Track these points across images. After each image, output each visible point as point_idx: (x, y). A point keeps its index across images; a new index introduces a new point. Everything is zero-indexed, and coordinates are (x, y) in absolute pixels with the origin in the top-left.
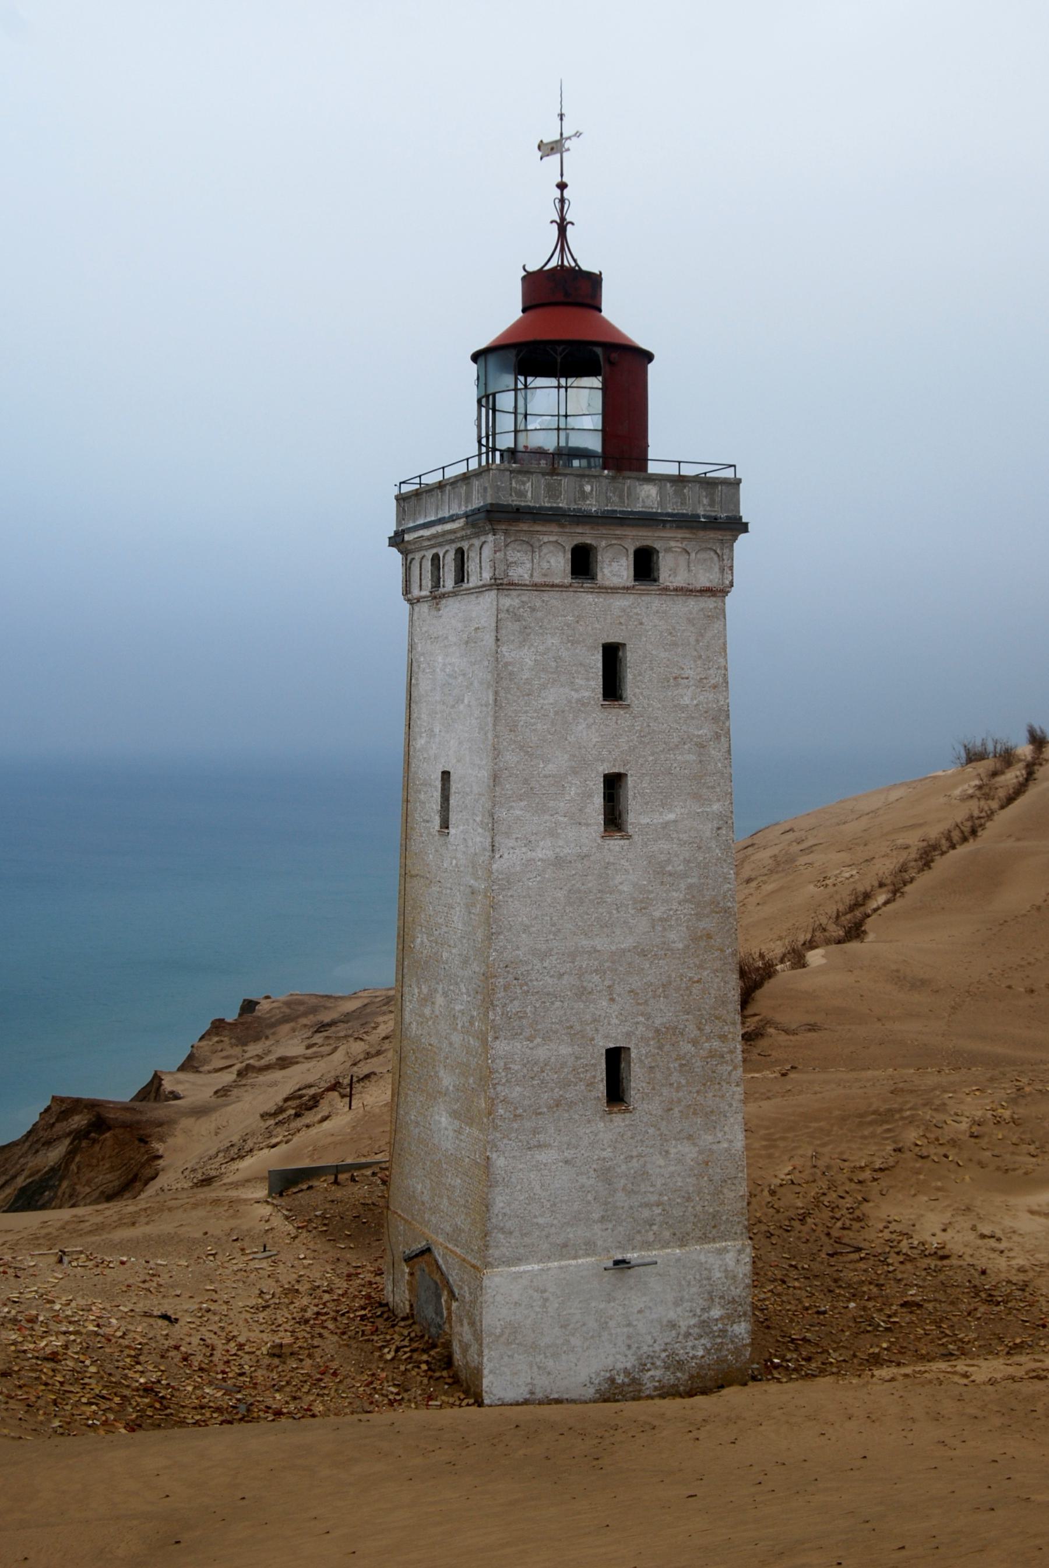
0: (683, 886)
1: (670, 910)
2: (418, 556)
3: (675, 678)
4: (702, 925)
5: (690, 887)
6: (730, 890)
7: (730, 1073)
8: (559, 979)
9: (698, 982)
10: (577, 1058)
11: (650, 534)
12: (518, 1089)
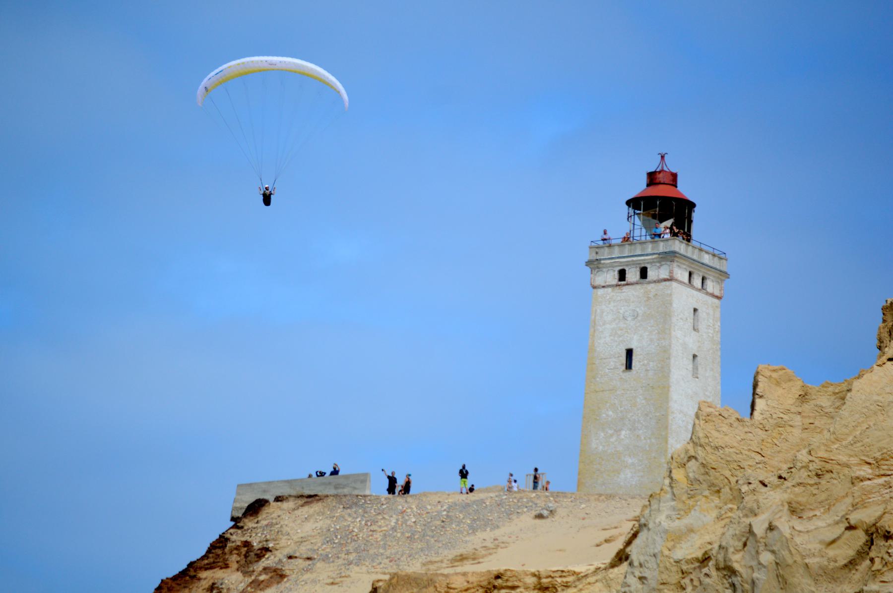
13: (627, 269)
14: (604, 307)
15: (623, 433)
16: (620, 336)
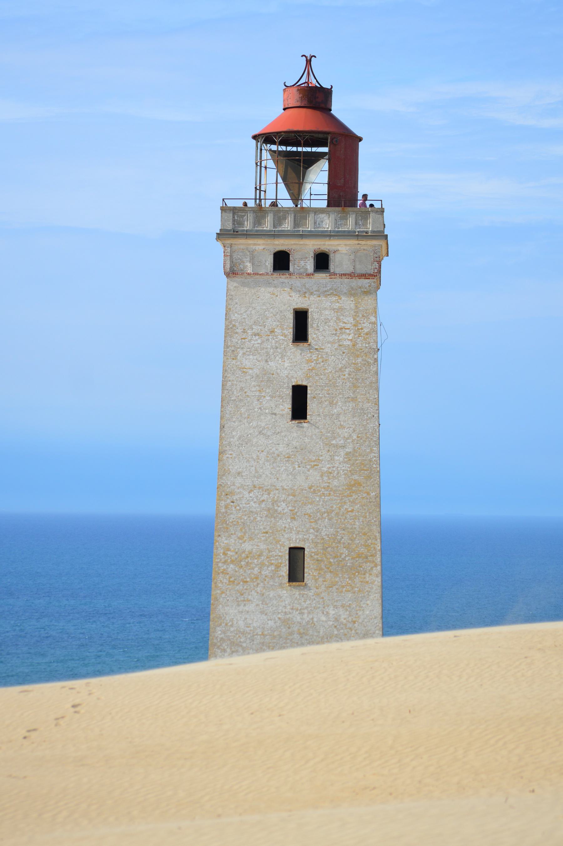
0: (342, 453)
1: (333, 467)
3: (341, 329)
4: (356, 477)
5: (347, 454)
6: (375, 457)
7: (372, 568)
8: (259, 504)
9: (351, 511)
10: (269, 551)
11: (323, 243)
12: (232, 566)
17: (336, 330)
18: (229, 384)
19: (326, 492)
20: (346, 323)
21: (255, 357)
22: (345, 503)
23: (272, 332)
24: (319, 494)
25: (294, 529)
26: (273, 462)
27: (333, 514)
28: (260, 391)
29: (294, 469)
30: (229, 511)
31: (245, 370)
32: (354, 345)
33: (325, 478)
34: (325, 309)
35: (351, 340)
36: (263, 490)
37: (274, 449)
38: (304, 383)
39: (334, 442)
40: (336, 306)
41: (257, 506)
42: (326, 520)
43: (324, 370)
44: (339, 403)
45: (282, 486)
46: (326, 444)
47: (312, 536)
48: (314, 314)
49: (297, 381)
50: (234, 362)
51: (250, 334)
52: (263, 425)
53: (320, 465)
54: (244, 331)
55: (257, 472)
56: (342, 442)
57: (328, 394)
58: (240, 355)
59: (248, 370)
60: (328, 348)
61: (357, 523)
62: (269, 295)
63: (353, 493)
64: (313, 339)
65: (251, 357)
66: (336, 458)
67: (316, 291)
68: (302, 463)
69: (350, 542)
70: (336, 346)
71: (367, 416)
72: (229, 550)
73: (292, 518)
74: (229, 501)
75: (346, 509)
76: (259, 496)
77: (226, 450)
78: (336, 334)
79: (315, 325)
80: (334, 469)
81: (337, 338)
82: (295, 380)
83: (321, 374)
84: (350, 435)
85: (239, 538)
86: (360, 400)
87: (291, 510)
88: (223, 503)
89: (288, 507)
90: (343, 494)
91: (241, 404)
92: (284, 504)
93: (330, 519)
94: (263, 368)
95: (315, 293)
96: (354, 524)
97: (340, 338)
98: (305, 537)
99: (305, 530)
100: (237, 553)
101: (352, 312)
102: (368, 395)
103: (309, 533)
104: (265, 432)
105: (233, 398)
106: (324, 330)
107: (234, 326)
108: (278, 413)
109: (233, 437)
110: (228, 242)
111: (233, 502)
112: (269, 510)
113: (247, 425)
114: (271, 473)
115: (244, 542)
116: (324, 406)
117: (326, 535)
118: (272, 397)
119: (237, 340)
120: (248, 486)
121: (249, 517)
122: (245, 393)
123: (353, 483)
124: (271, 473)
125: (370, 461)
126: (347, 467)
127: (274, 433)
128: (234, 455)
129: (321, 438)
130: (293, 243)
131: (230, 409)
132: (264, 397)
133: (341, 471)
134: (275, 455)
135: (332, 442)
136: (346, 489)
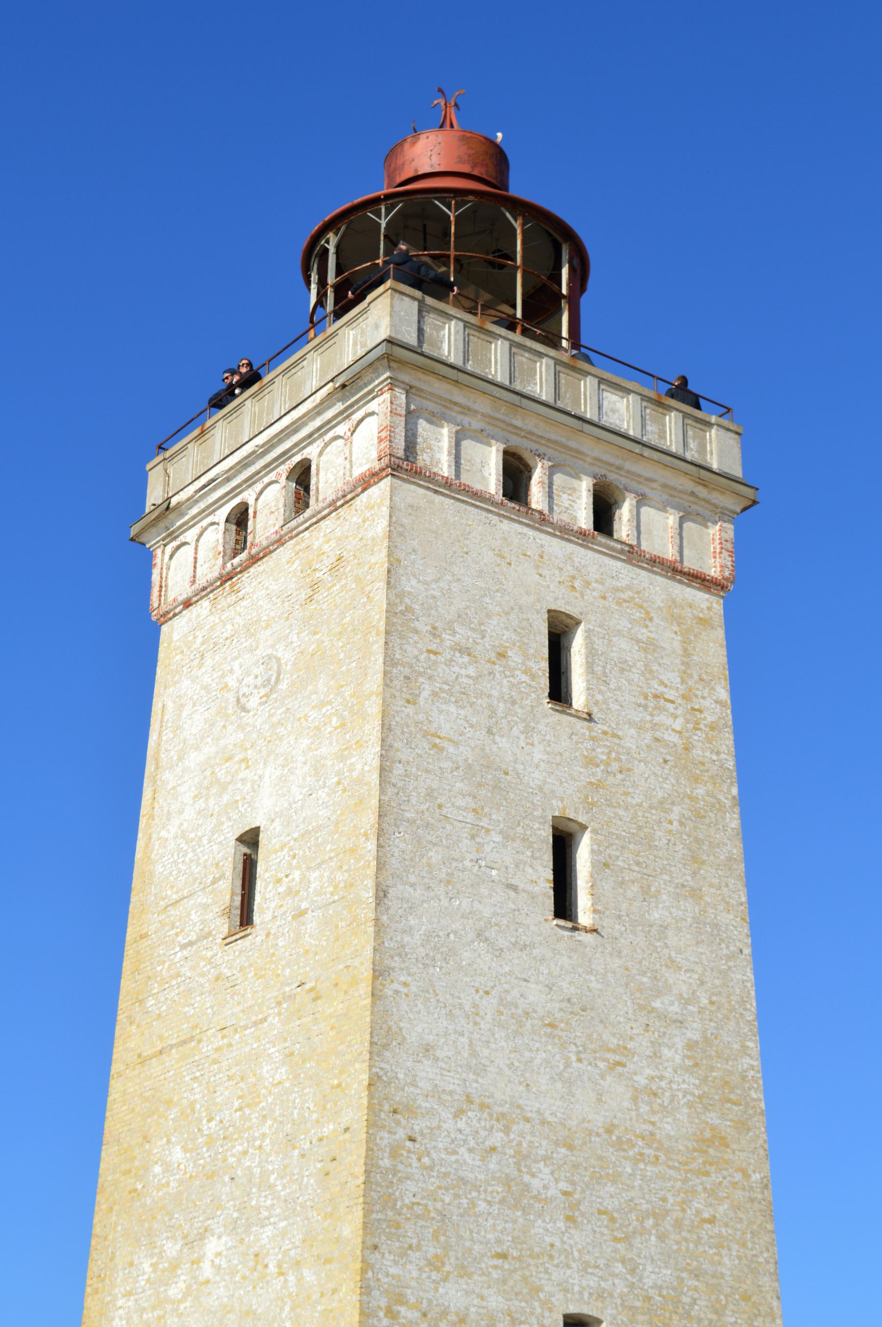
0: (679, 1042)
1: (661, 1078)
2: (190, 535)
3: (656, 696)
4: (713, 1118)
5: (691, 1045)
13: (251, 502)
14: (186, 683)
15: (212, 1246)
16: (224, 788)
17: (646, 698)
18: (398, 770)
19: (647, 1151)
20: (666, 686)
21: (462, 712)
22: (694, 1192)
23: (502, 655)
24: (631, 1153)
25: (576, 1254)
26: (516, 1033)
27: (667, 1224)
28: (474, 810)
29: (567, 1065)
30: (400, 1167)
31: (438, 741)
32: (687, 749)
33: (644, 1109)
34: (619, 633)
35: (680, 732)
36: (491, 1115)
37: (515, 993)
38: (582, 819)
39: (657, 1004)
40: (643, 634)
41: (478, 1163)
42: (653, 1238)
43: (626, 794)
44: (664, 897)
45: (538, 1112)
46: (642, 1008)
47: (621, 1288)
48: (596, 639)
49: (564, 809)
50: (410, 710)
51: (448, 643)
52: (487, 912)
53: (631, 1067)
54: (434, 632)
55: (474, 1054)
56: (675, 1008)
57: (638, 864)
58: (425, 694)
59: (445, 744)
60: (630, 739)
61: (726, 1260)
62: (491, 553)
63: (711, 1164)
64: (596, 703)
65: (452, 708)
66: (665, 1051)
67: (597, 581)
68: (585, 1050)
69: (714, 1317)
70: (648, 738)
71: (728, 947)
72: (400, 1299)
73: (570, 1219)
74: (401, 1134)
75: (698, 1212)
76: (483, 1133)
77: (393, 969)
78: (646, 707)
79: (598, 669)
80: (663, 1084)
81: (648, 718)
82: (560, 804)
83: (619, 806)
84: (694, 992)
85: (430, 1263)
86: (708, 899)
87: (565, 1193)
88: (385, 1139)
89: (557, 1181)
90: (686, 1164)
91: (429, 838)
92: (547, 1170)
93: (662, 1237)
94: (483, 750)
95: (594, 585)
96: (720, 1263)
97: (657, 719)
98: (603, 1284)
99: (601, 1262)
100: (425, 1315)
101: (678, 661)
102: (725, 890)
103: (614, 1275)
104: (491, 934)
105: (408, 815)
106: (619, 689)
107: (409, 609)
108: (521, 886)
109: (409, 931)
110: (406, 377)
111: (412, 1139)
112: (507, 1182)
113: (445, 903)
114: (511, 1066)
115: (445, 1279)
116: (629, 894)
117: (655, 1286)
118: (507, 837)
119: (416, 652)
120: (451, 1093)
121: (457, 1196)
122: (440, 806)
123: (708, 1134)
124: (511, 1066)
125: (744, 1078)
126: (690, 1082)
127: (514, 944)
128: (414, 989)
129: (627, 985)
130: (553, 437)
131: (402, 846)
132: (488, 831)
133: (680, 1095)
134: (520, 1011)
135: (654, 1005)
136: (695, 1150)
